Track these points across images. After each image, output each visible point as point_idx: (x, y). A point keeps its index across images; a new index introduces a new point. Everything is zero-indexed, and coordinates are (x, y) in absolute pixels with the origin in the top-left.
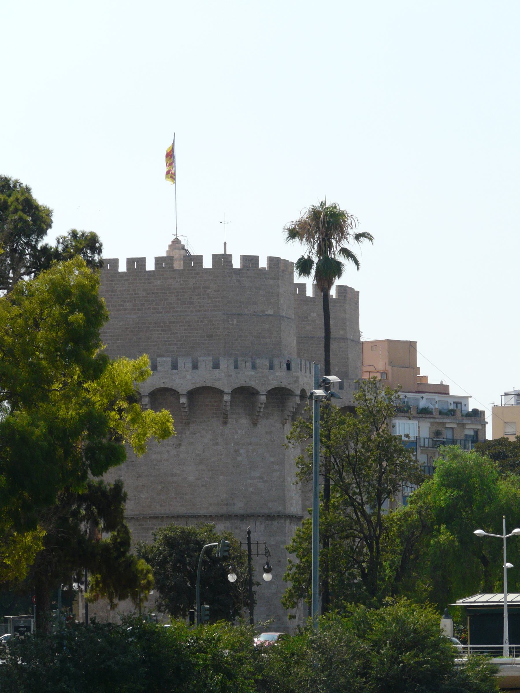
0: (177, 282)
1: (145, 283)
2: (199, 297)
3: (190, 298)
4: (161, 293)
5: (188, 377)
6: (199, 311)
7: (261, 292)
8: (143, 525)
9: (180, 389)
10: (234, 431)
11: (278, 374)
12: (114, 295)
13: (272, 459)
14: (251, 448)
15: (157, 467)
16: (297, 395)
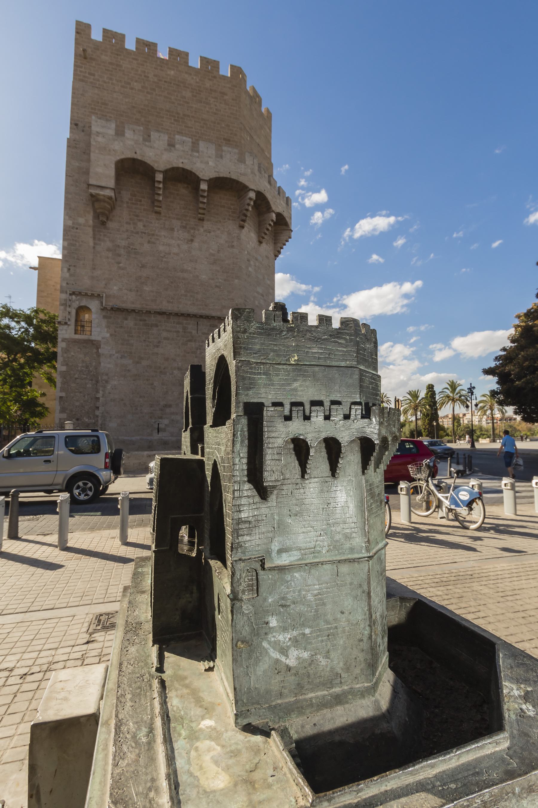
0: (193, 78)
5: (211, 163)
8: (145, 320)
9: (201, 173)
12: (120, 70)
15: (164, 259)
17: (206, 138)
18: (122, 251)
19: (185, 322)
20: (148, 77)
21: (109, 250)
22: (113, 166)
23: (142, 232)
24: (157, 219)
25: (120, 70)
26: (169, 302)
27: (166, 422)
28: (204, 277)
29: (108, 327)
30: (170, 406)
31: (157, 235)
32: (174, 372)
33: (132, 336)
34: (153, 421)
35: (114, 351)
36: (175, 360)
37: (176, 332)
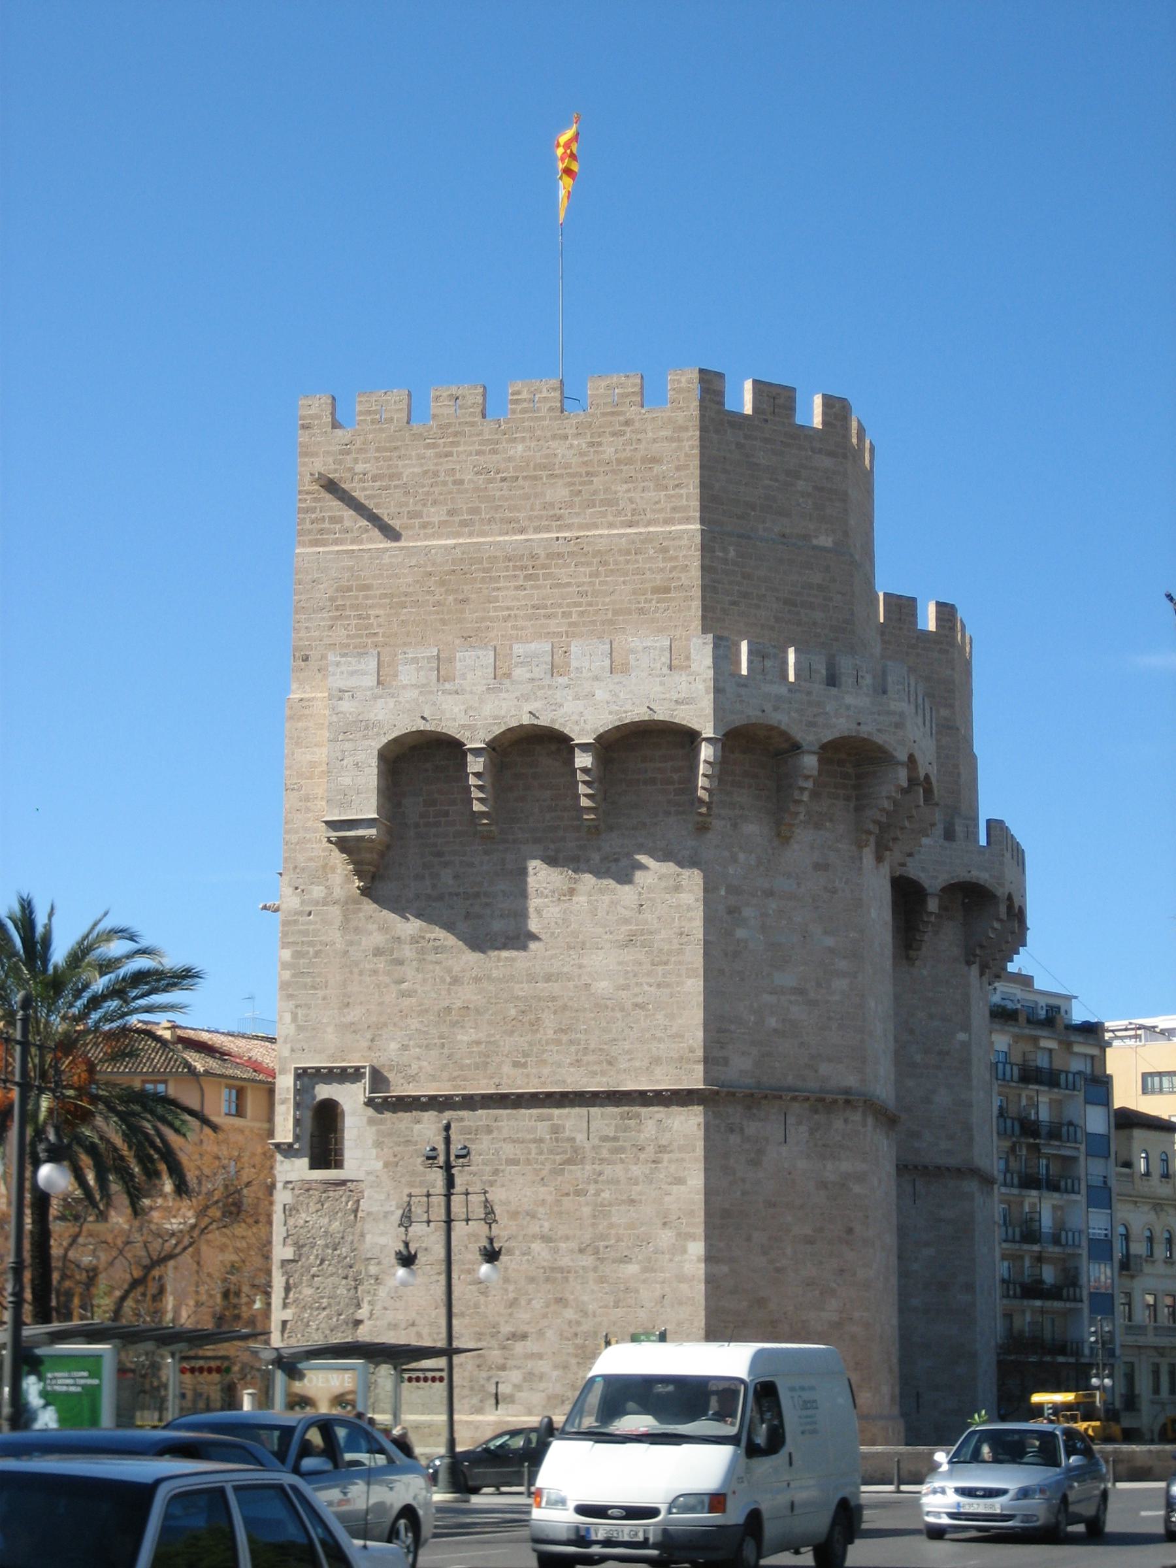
0: (571, 446)
1: (478, 453)
2: (630, 485)
3: (606, 490)
7: (801, 485)
9: (577, 728)
10: (726, 854)
11: (849, 700)
13: (830, 942)
14: (774, 906)
16: (902, 764)
17: (607, 600)
18: (408, 952)
21: (378, 952)
22: (374, 762)
23: (450, 894)
24: (486, 853)
26: (516, 1065)
27: (515, 1376)
28: (604, 984)
29: (378, 1144)
30: (524, 1337)
31: (486, 894)
32: (533, 1246)
34: (484, 1374)
35: (394, 1203)
36: (533, 1215)
37: (535, 1141)
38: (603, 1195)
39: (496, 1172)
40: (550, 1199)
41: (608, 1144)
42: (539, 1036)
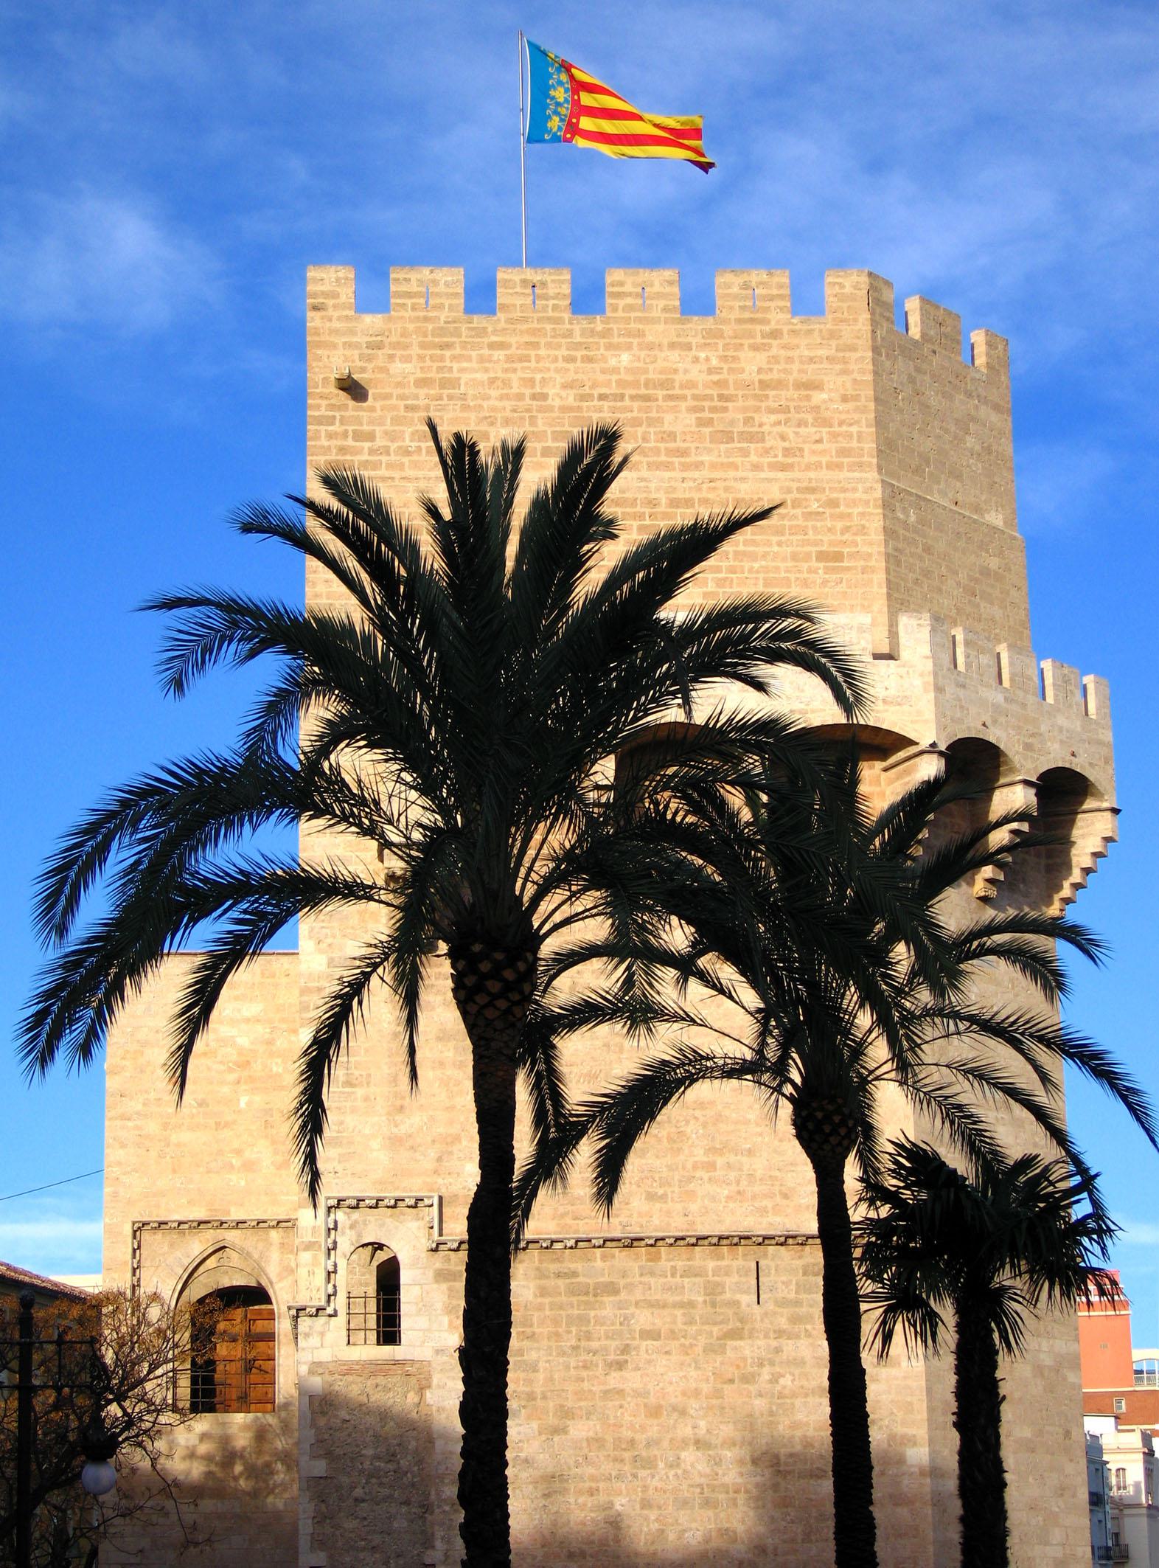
0: (696, 360)
1: (571, 359)
2: (782, 417)
3: (748, 421)
4: (633, 398)
6: (784, 468)
8: (574, 1274)
12: (450, 398)
17: (756, 565)
19: (711, 1264)
20: (544, 397)
25: (450, 398)
26: (651, 1197)
32: (683, 1455)
33: (534, 1334)
36: (683, 1413)
37: (681, 1305)
38: (782, 1381)
39: (626, 1349)
40: (706, 1388)
41: (786, 1311)
42: (682, 1157)
